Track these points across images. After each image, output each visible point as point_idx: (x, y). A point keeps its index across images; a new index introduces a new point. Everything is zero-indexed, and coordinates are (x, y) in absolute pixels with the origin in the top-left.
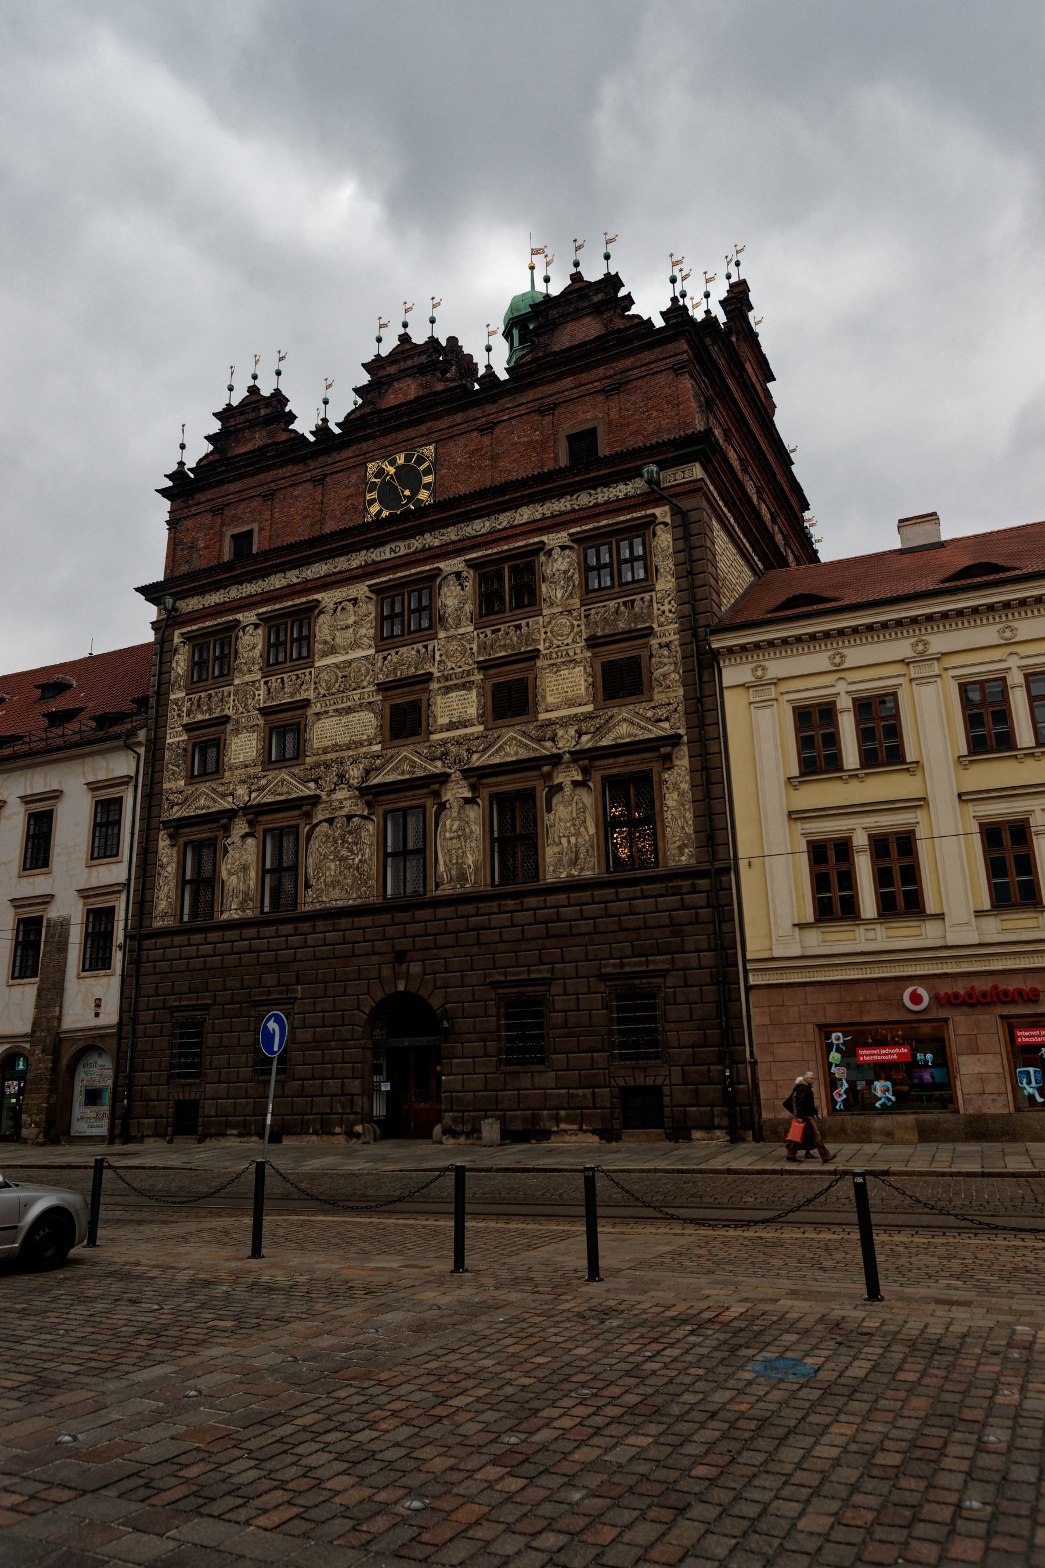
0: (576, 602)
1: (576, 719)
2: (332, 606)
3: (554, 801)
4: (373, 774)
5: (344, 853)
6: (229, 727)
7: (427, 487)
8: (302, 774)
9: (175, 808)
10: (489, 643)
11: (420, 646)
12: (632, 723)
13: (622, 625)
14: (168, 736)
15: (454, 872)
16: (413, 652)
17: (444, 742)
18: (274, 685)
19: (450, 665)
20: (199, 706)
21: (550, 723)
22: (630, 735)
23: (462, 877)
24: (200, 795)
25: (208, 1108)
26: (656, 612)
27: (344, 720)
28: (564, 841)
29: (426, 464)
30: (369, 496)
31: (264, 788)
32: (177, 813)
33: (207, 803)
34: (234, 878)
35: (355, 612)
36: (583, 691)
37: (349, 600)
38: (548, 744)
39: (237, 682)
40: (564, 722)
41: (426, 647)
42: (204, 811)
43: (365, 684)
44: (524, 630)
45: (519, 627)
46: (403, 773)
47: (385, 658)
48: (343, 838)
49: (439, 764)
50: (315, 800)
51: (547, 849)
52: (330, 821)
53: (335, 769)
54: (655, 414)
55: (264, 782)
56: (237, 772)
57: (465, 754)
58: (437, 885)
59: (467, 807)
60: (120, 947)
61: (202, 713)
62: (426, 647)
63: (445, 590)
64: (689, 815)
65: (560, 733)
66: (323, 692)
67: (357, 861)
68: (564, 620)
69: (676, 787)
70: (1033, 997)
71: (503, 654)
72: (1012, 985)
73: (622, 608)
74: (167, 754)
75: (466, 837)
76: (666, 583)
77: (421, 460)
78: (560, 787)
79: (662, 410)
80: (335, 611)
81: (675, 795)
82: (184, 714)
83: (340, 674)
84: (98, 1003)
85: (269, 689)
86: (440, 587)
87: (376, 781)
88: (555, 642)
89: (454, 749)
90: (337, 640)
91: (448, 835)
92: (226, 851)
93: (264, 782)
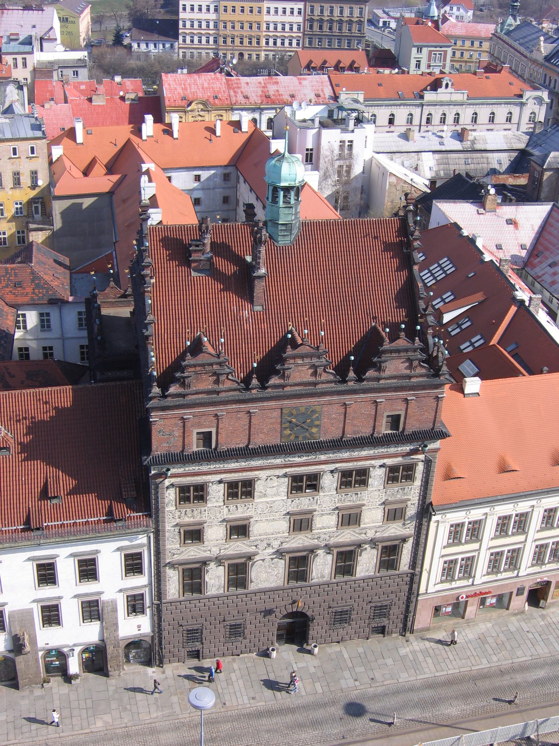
0: (382, 487)
1: (375, 527)
2: (265, 477)
3: (363, 553)
4: (284, 544)
5: (270, 570)
6: (205, 525)
7: (318, 426)
8: (248, 544)
9: (175, 556)
10: (343, 499)
11: (310, 498)
12: (396, 529)
13: (398, 496)
14: (167, 526)
15: (319, 576)
16: (307, 500)
17: (319, 533)
18: (232, 508)
19: (324, 506)
20: (185, 514)
21: (365, 528)
22: (395, 533)
23: (323, 576)
24: (190, 551)
25: (206, 651)
26: (412, 493)
27: (270, 524)
28: (364, 565)
29: (317, 415)
30: (283, 426)
31: (228, 548)
32: (176, 558)
33: (195, 554)
34: (213, 581)
35: (278, 481)
36: (380, 518)
37: (275, 476)
38: (364, 535)
39: (209, 505)
40: (370, 528)
41: (313, 498)
42: (193, 557)
43: (282, 510)
44: (359, 495)
45: (357, 494)
46: (299, 544)
47: (292, 501)
48: (270, 566)
49: (316, 540)
50: (256, 554)
51: (358, 568)
52: (263, 560)
53: (265, 542)
54: (426, 413)
55: (228, 546)
56: (211, 542)
57: (328, 538)
58: (312, 580)
59: (328, 555)
60: (149, 607)
61: (188, 517)
62: (313, 498)
63: (324, 477)
64: (410, 556)
65: (368, 531)
66: (259, 512)
67: (276, 573)
68: (377, 493)
69: (407, 548)
70: (490, 592)
71: (349, 504)
72: (487, 591)
73: (400, 490)
74: (167, 534)
75: (325, 565)
76: (418, 483)
77: (313, 412)
78: (366, 549)
79: (429, 413)
80: (267, 480)
81: (406, 551)
82: (177, 517)
83: (269, 506)
84: (139, 626)
85: (229, 510)
86: (323, 475)
87: (285, 546)
88: (372, 501)
89: (323, 536)
90: (267, 492)
91: (318, 564)
92: (208, 571)
93: (228, 546)
